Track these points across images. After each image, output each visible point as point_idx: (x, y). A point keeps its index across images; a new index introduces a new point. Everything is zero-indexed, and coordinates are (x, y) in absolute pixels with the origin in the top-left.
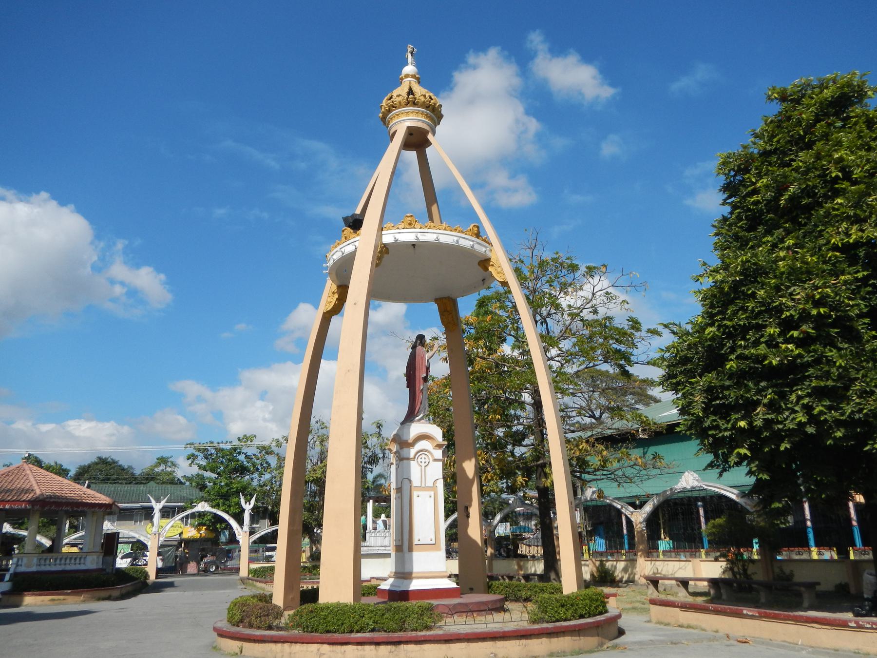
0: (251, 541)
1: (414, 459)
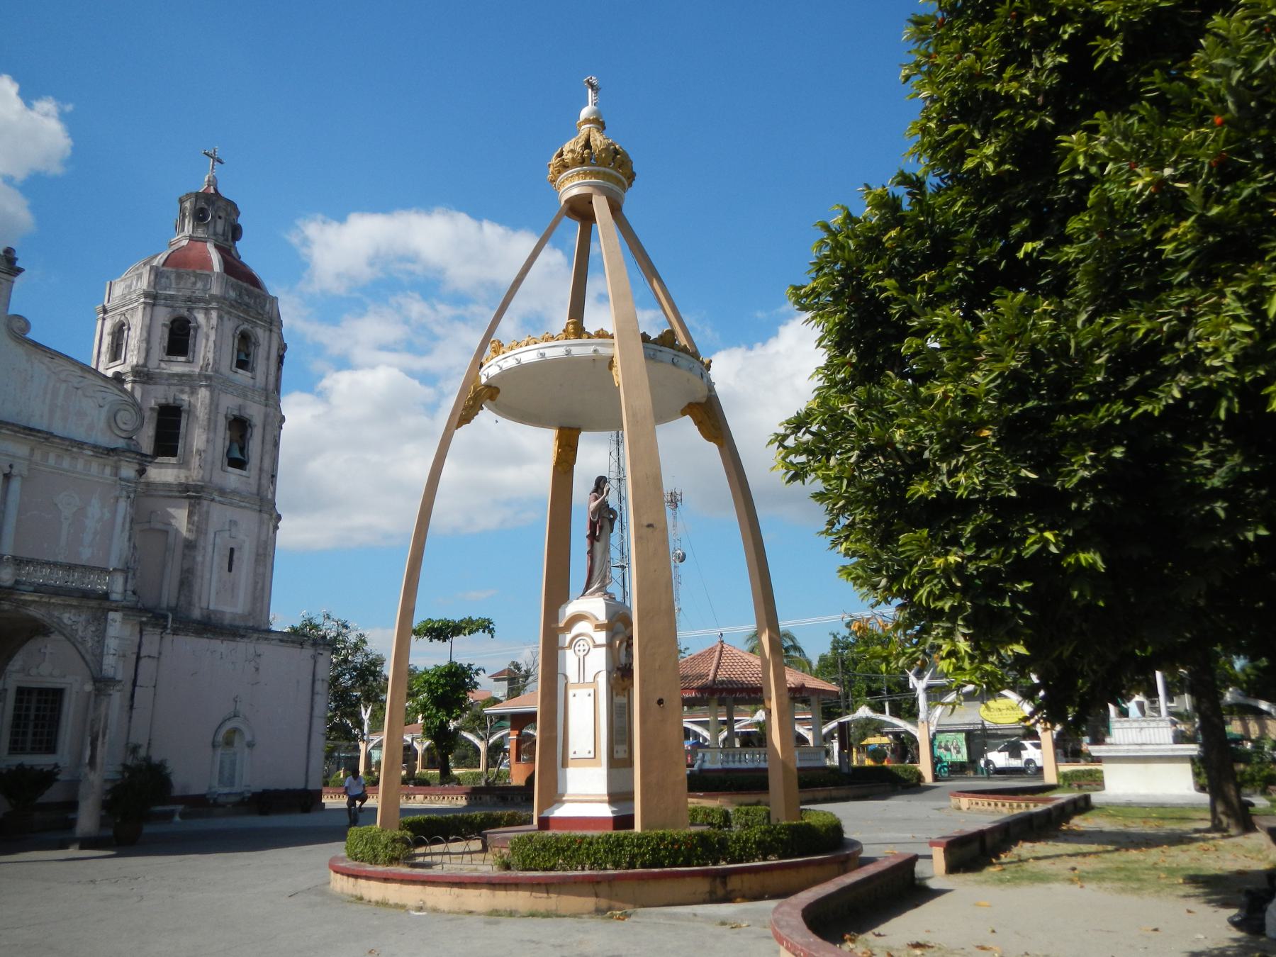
1: (570, 647)
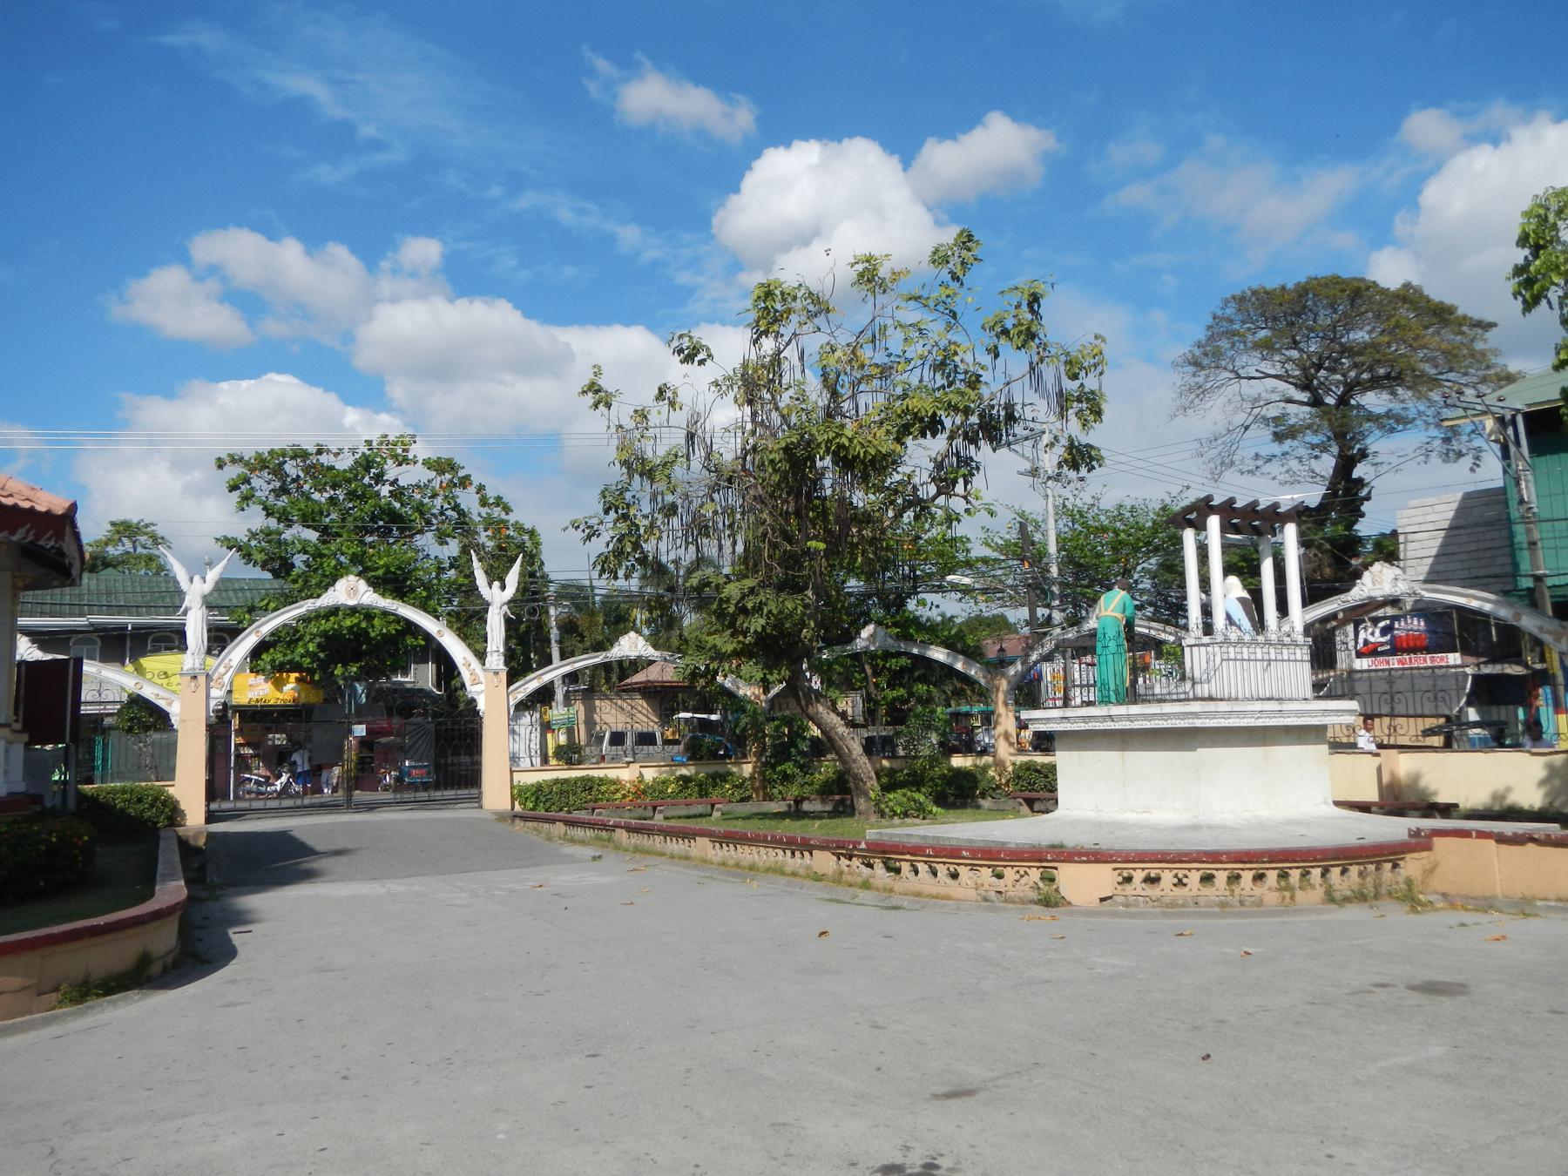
0: (513, 702)
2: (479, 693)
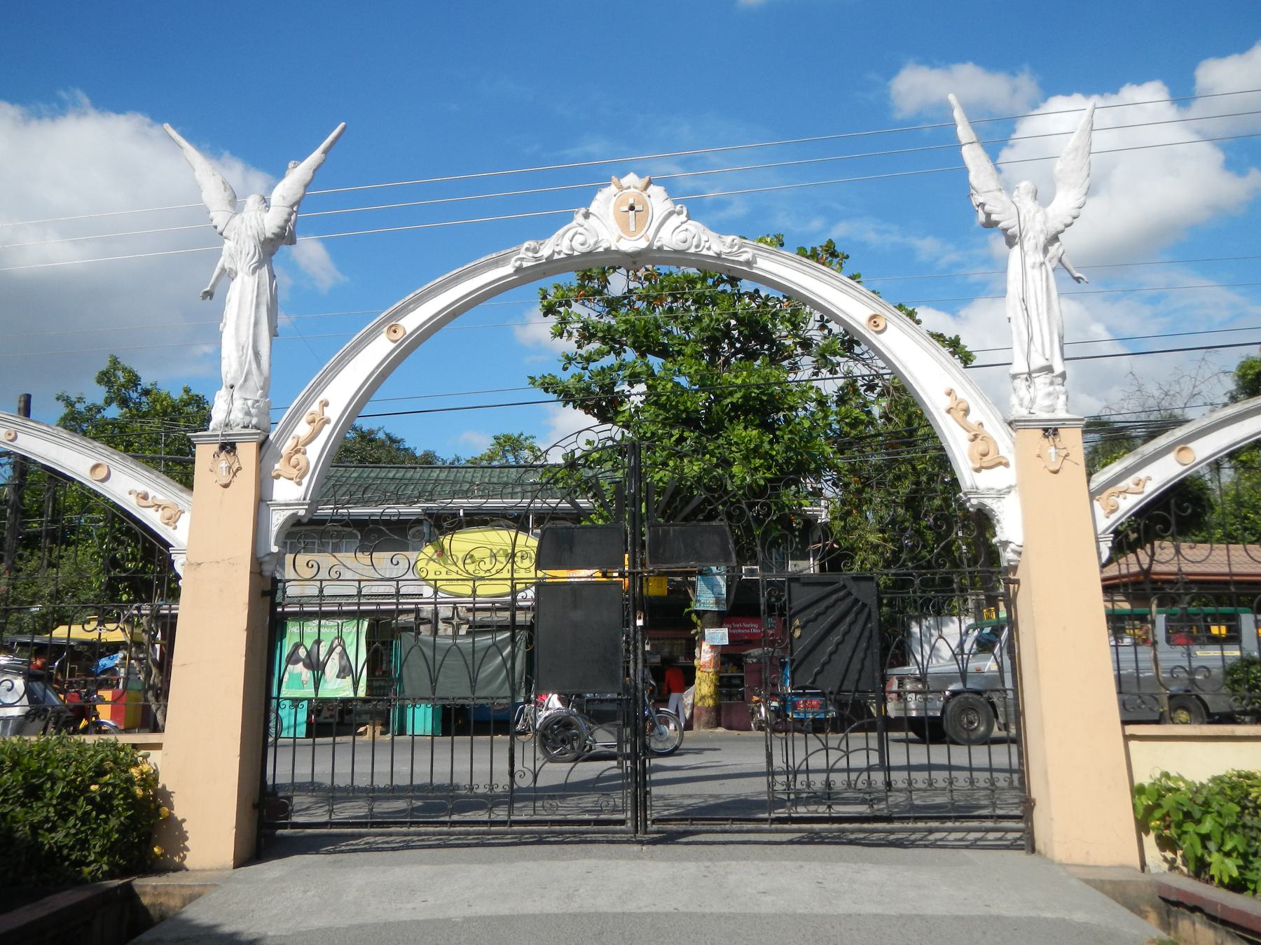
0: (1105, 522)
2: (1000, 494)
